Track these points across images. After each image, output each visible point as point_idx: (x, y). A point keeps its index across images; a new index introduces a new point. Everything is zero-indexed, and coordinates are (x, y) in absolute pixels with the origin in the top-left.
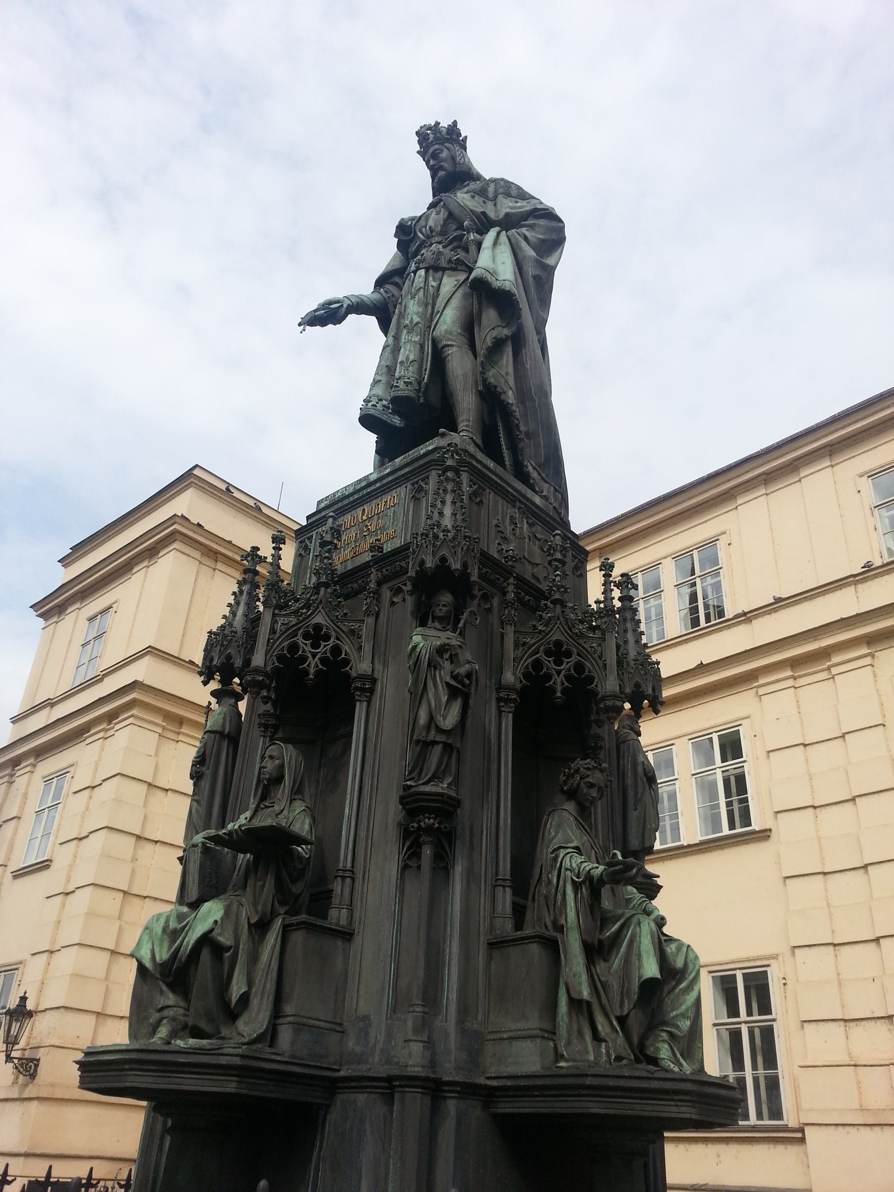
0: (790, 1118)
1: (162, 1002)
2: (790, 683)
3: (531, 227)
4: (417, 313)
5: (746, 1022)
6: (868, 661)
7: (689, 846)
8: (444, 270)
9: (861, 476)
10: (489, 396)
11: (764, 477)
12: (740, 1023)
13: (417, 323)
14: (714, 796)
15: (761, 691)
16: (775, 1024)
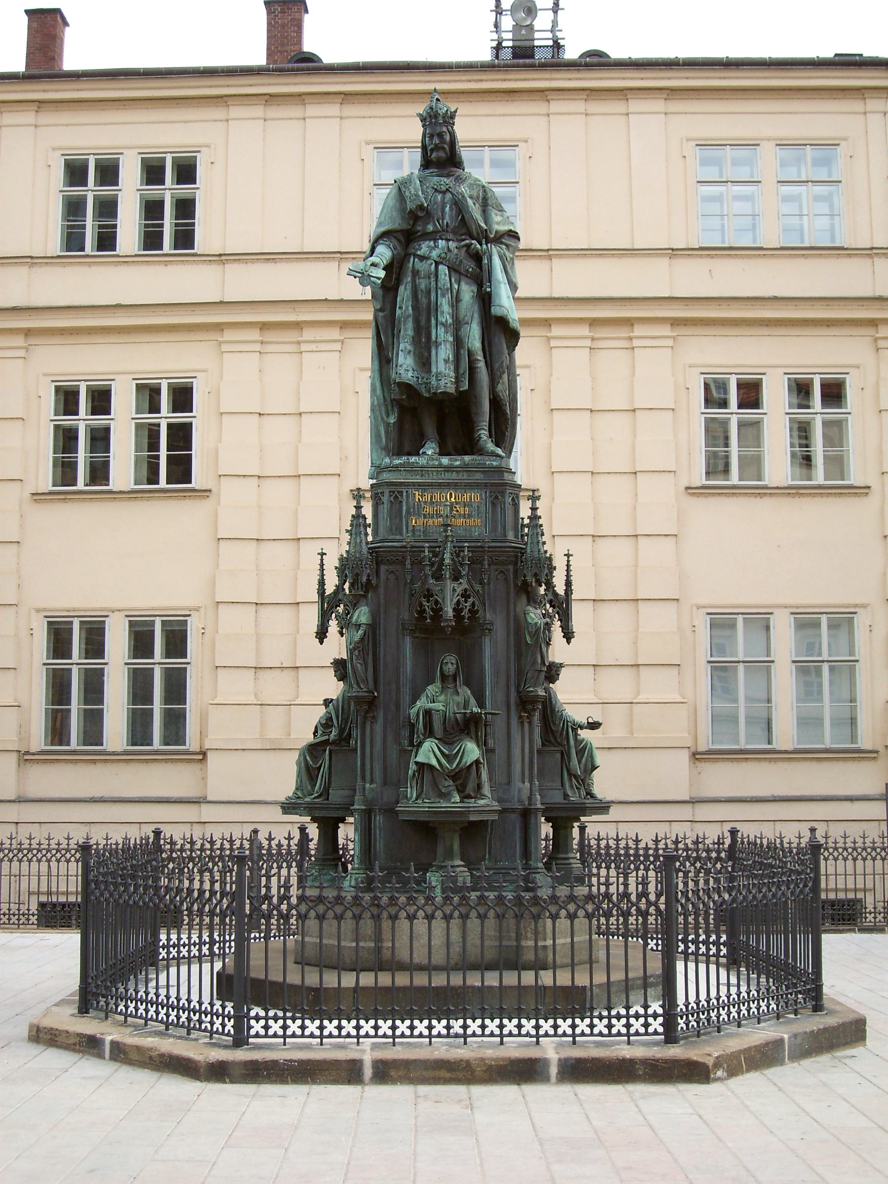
0: (192, 742)
1: (447, 784)
2: (257, 347)
3: (507, 246)
4: (449, 314)
5: (159, 663)
6: (338, 346)
7: (121, 492)
8: (460, 274)
9: (368, 143)
10: (496, 403)
11: (267, 97)
12: (154, 664)
13: (450, 325)
14: (154, 445)
15: (225, 348)
16: (188, 667)
